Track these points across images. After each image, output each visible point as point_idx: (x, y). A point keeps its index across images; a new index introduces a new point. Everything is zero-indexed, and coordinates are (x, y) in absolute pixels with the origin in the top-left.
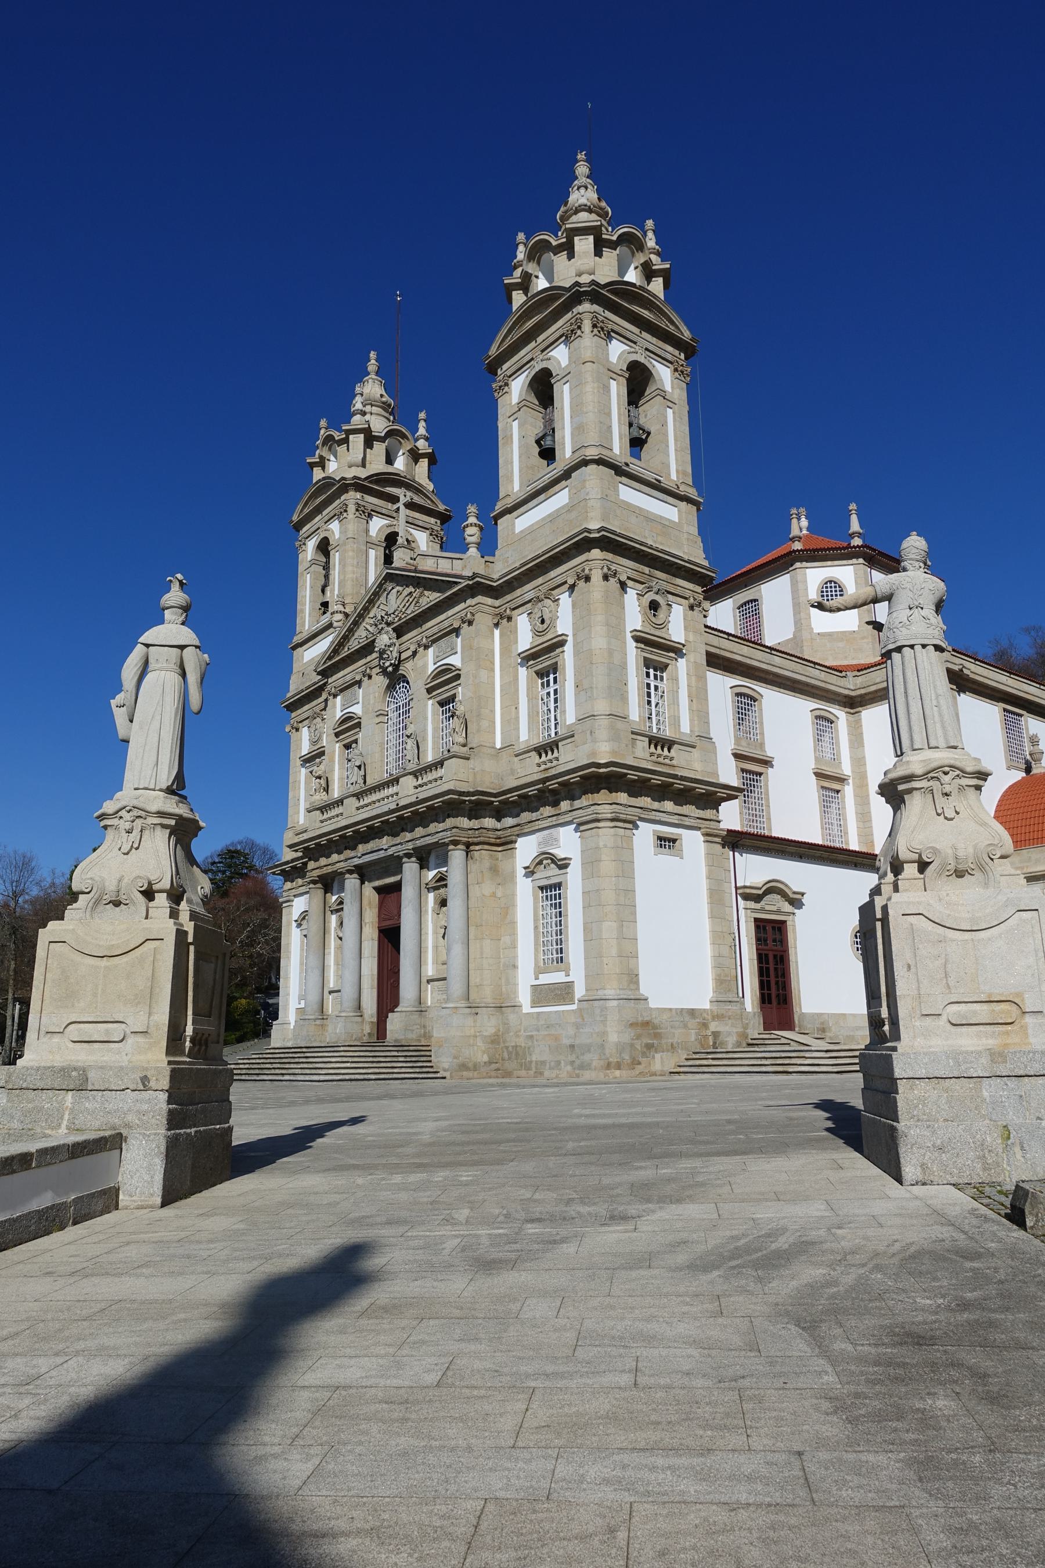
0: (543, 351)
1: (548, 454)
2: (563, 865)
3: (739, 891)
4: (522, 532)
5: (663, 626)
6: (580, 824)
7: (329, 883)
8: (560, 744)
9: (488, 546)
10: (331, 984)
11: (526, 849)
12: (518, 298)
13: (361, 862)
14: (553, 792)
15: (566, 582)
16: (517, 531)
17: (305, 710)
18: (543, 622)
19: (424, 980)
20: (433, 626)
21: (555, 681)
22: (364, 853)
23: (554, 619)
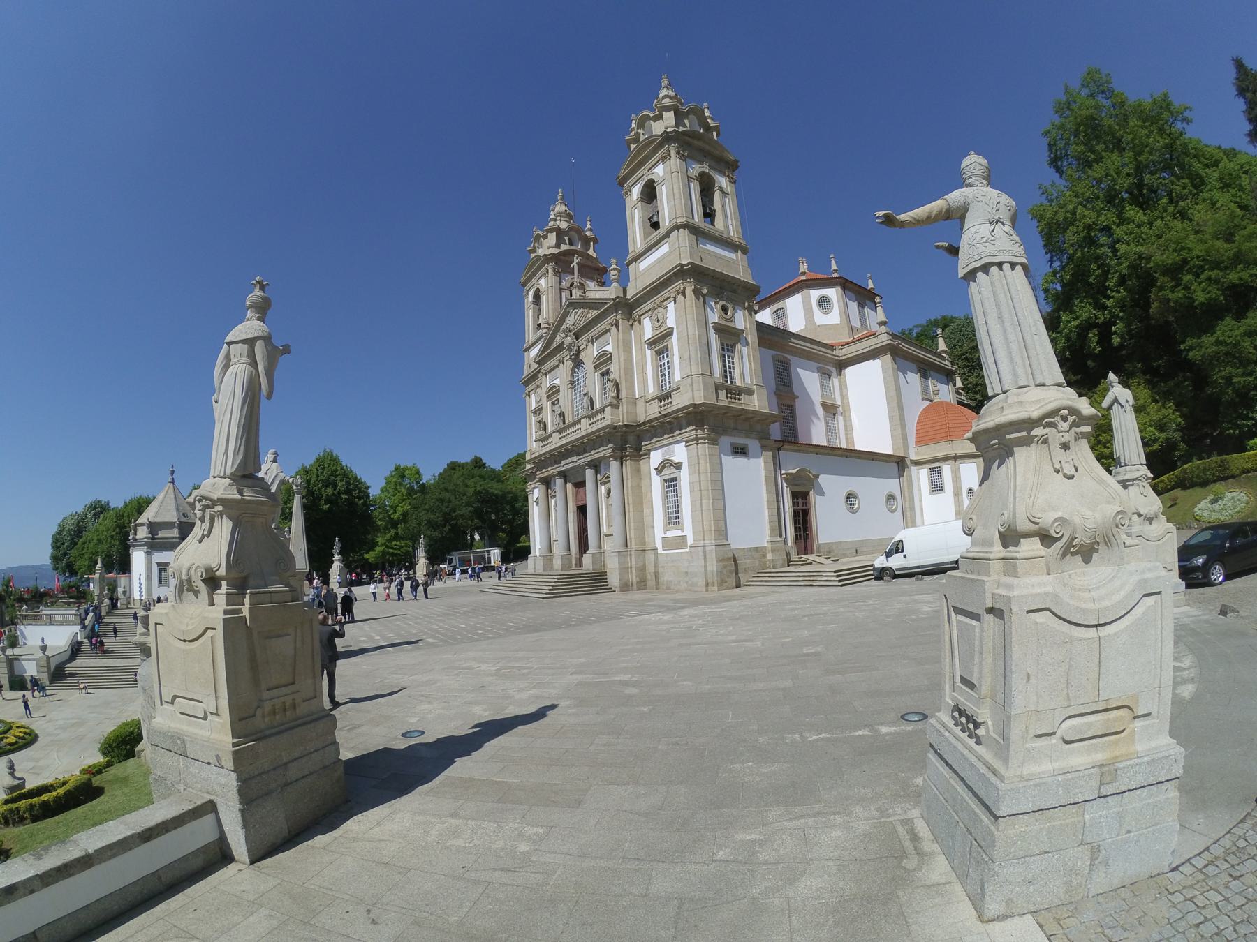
0: (649, 170)
1: (655, 225)
2: (678, 466)
3: (783, 476)
4: (643, 270)
5: (732, 320)
6: (686, 442)
7: (547, 482)
8: (672, 394)
9: (624, 280)
11: (656, 458)
12: (632, 147)
14: (669, 423)
15: (670, 297)
16: (640, 270)
17: (532, 386)
20: (595, 331)
21: (667, 356)
22: (565, 465)
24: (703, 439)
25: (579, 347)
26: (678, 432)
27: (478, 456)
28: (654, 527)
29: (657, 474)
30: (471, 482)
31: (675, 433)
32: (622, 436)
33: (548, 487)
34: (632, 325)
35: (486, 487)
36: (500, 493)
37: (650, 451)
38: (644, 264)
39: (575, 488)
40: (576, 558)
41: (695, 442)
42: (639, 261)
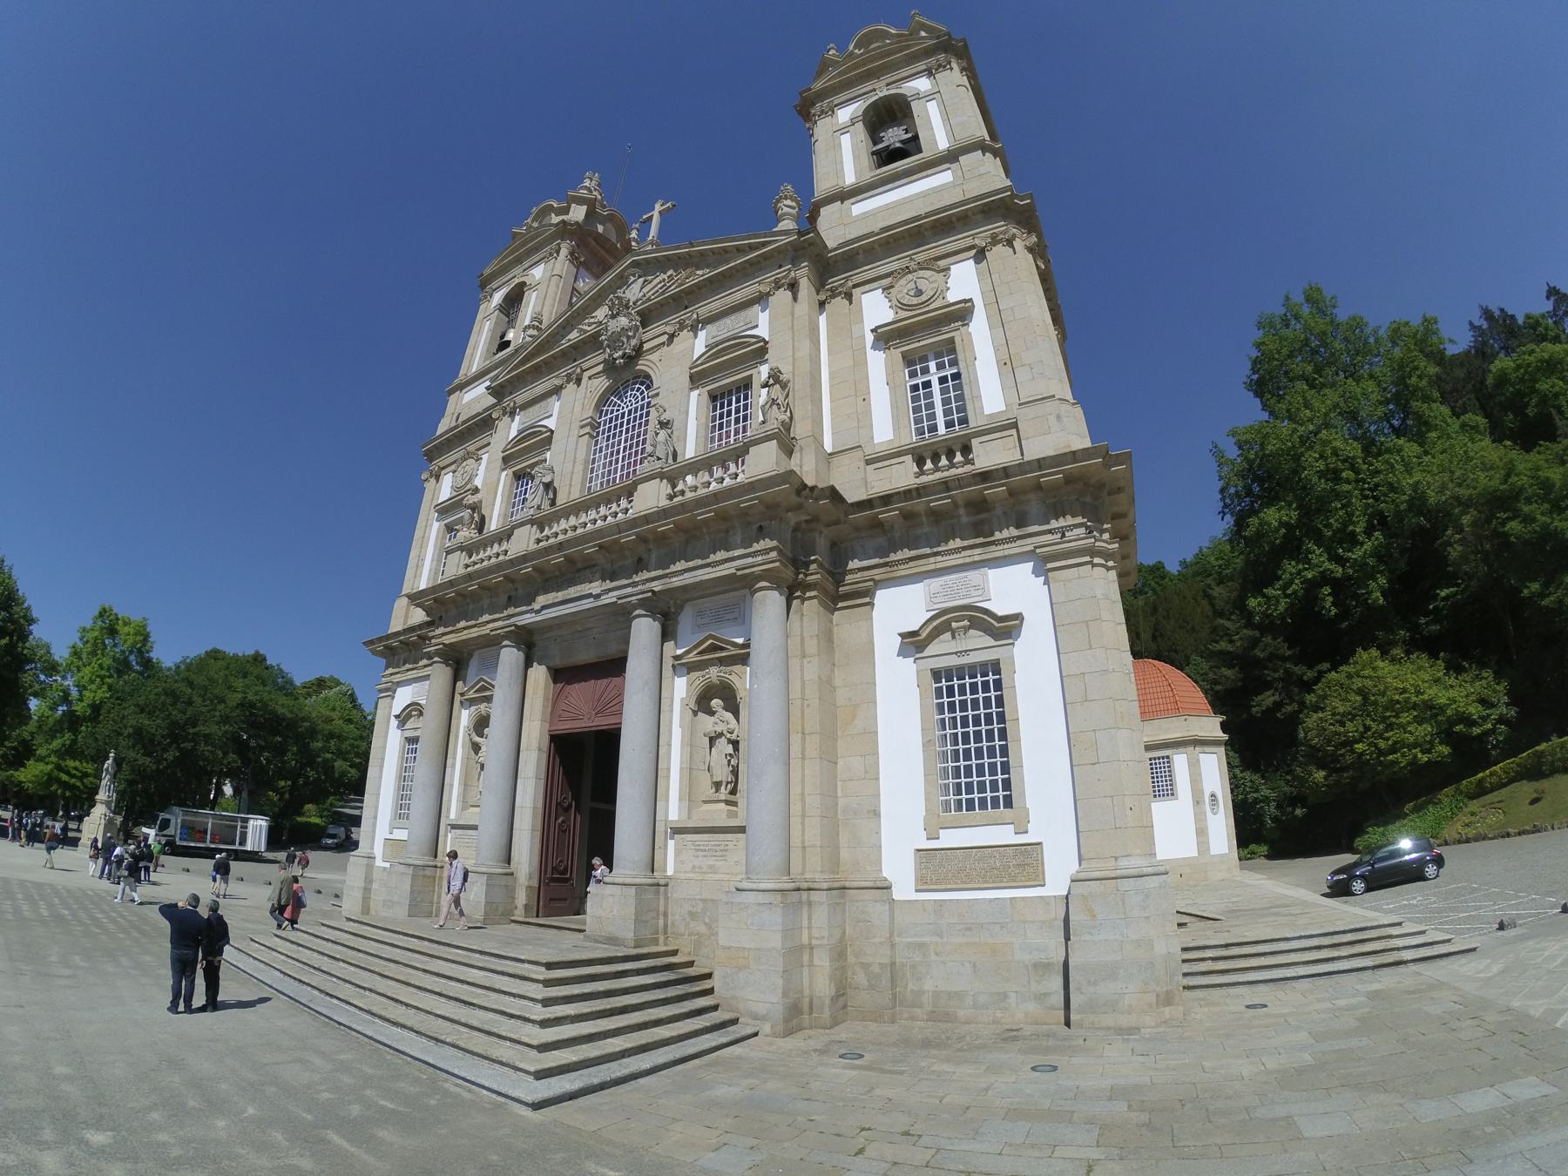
7: (457, 661)
8: (975, 442)
10: (453, 812)
13: (539, 618)
18: (919, 293)
19: (660, 827)
21: (940, 367)
22: (546, 608)
23: (941, 292)
24: (1107, 555)
25: (642, 344)
26: (1014, 532)
27: (262, 652)
28: (876, 814)
29: (903, 652)
30: (239, 683)
31: (998, 535)
32: (796, 529)
33: (458, 674)
34: (822, 304)
35: (266, 697)
36: (289, 715)
37: (879, 584)
38: (859, 208)
39: (555, 681)
40: (529, 888)
41: (1087, 559)
42: (853, 200)
